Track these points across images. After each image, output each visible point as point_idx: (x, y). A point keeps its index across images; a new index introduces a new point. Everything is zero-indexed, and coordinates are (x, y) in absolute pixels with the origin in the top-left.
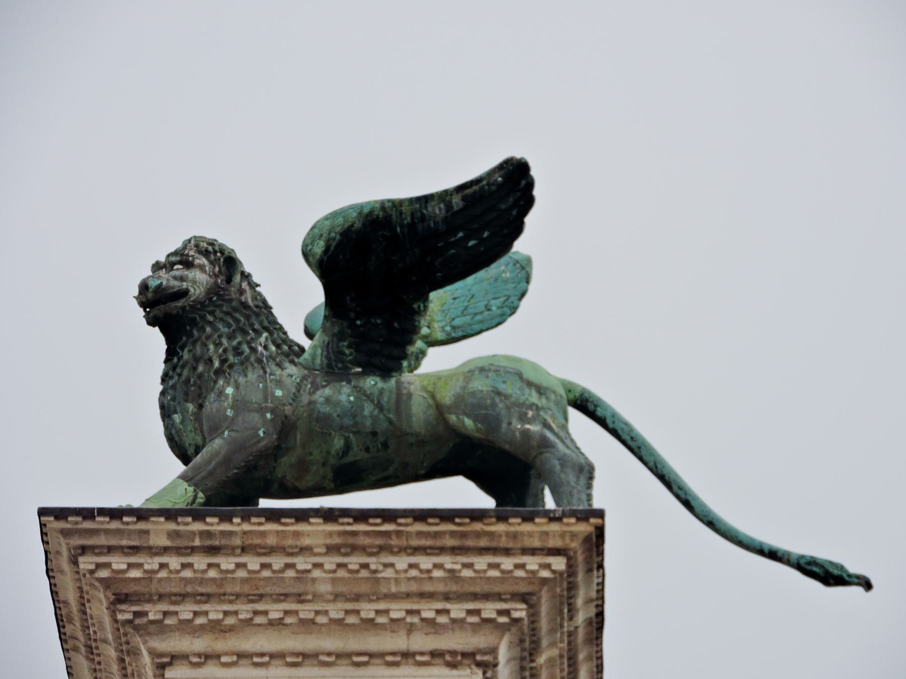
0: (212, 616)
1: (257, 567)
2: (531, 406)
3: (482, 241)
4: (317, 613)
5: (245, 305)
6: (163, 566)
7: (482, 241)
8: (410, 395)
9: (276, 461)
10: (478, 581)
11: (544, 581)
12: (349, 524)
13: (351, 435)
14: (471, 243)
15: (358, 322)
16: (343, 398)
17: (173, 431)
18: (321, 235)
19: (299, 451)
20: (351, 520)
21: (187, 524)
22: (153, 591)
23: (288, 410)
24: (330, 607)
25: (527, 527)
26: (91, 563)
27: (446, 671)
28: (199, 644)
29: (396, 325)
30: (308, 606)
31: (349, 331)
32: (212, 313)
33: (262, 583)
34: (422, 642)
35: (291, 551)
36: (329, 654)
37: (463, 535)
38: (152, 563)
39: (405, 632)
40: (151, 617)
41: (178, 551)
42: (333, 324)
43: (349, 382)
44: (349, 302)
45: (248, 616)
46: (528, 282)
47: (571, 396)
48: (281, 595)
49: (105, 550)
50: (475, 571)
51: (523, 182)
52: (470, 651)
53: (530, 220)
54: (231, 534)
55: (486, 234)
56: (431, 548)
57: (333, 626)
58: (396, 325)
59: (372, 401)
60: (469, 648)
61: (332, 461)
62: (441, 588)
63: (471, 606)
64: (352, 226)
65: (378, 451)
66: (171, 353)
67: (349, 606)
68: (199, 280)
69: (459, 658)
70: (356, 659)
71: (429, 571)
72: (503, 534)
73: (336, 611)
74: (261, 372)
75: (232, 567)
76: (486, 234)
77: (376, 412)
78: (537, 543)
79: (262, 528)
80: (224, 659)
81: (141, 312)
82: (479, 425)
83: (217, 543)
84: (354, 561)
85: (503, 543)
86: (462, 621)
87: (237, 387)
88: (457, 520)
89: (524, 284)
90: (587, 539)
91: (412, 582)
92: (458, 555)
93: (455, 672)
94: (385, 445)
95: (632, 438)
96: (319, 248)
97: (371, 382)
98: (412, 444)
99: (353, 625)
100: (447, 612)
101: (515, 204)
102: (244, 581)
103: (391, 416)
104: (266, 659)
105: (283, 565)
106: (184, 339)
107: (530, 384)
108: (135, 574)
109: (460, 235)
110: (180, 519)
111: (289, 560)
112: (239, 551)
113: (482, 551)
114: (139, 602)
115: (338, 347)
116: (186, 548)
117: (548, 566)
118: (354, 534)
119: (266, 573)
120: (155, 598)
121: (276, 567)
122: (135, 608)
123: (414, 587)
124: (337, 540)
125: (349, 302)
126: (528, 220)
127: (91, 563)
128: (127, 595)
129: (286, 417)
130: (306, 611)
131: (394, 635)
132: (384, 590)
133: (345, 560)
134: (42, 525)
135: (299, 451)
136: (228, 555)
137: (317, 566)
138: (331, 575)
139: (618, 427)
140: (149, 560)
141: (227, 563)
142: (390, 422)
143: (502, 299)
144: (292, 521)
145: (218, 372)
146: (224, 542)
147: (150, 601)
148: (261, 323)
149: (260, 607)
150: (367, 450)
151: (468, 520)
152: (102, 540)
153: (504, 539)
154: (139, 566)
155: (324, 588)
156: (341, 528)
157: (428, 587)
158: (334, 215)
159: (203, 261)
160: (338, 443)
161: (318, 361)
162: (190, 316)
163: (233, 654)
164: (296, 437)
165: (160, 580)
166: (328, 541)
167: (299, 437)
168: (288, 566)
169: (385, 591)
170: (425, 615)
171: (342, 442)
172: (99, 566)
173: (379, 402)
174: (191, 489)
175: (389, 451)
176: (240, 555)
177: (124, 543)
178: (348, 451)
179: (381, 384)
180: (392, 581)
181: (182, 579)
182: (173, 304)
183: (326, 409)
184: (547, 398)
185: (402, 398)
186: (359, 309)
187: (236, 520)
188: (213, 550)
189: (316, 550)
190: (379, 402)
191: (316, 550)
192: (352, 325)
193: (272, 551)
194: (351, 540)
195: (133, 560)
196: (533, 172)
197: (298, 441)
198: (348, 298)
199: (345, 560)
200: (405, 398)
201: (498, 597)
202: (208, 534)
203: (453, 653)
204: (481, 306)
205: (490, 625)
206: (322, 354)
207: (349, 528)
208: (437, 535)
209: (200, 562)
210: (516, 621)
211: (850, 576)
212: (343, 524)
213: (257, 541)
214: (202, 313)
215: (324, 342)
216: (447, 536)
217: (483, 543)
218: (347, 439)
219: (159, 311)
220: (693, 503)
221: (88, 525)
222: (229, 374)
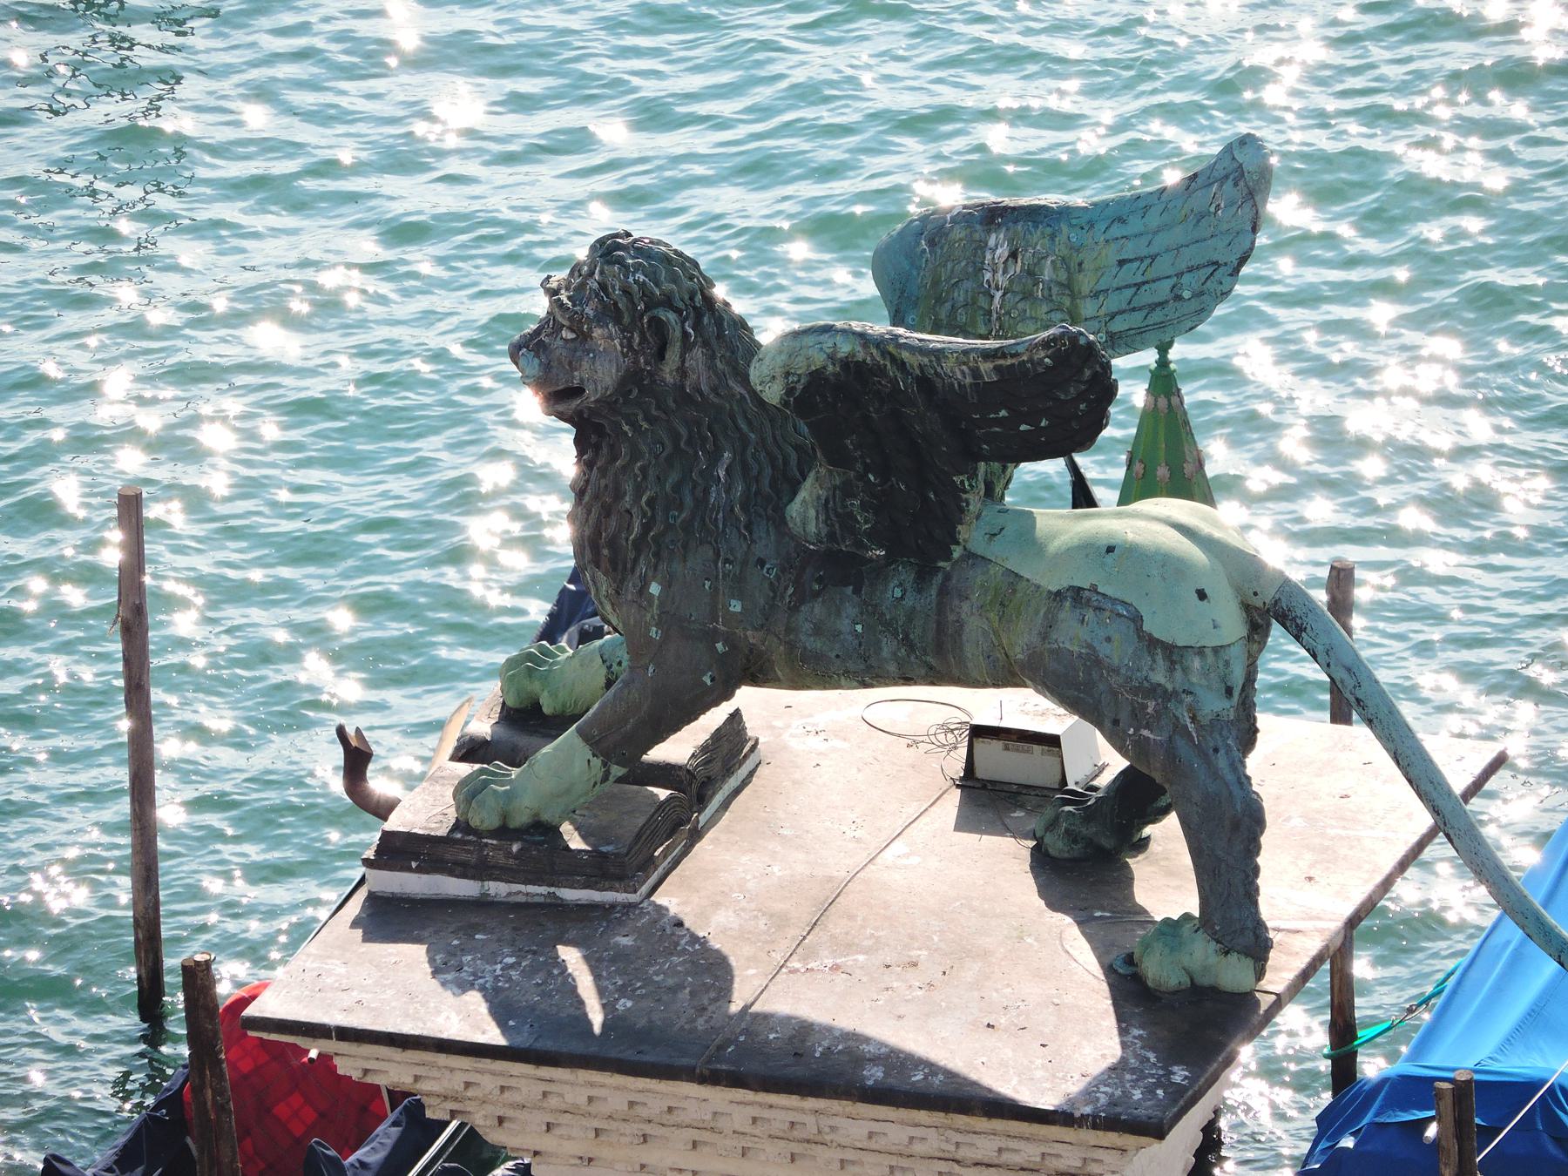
2: (1154, 690)
16: (844, 625)
23: (753, 637)
59: (895, 635)
87: (667, 585)
89: (1250, 235)
103: (929, 659)
161: (812, 528)
173: (906, 637)
174: (597, 762)
190: (906, 637)
215: (819, 498)
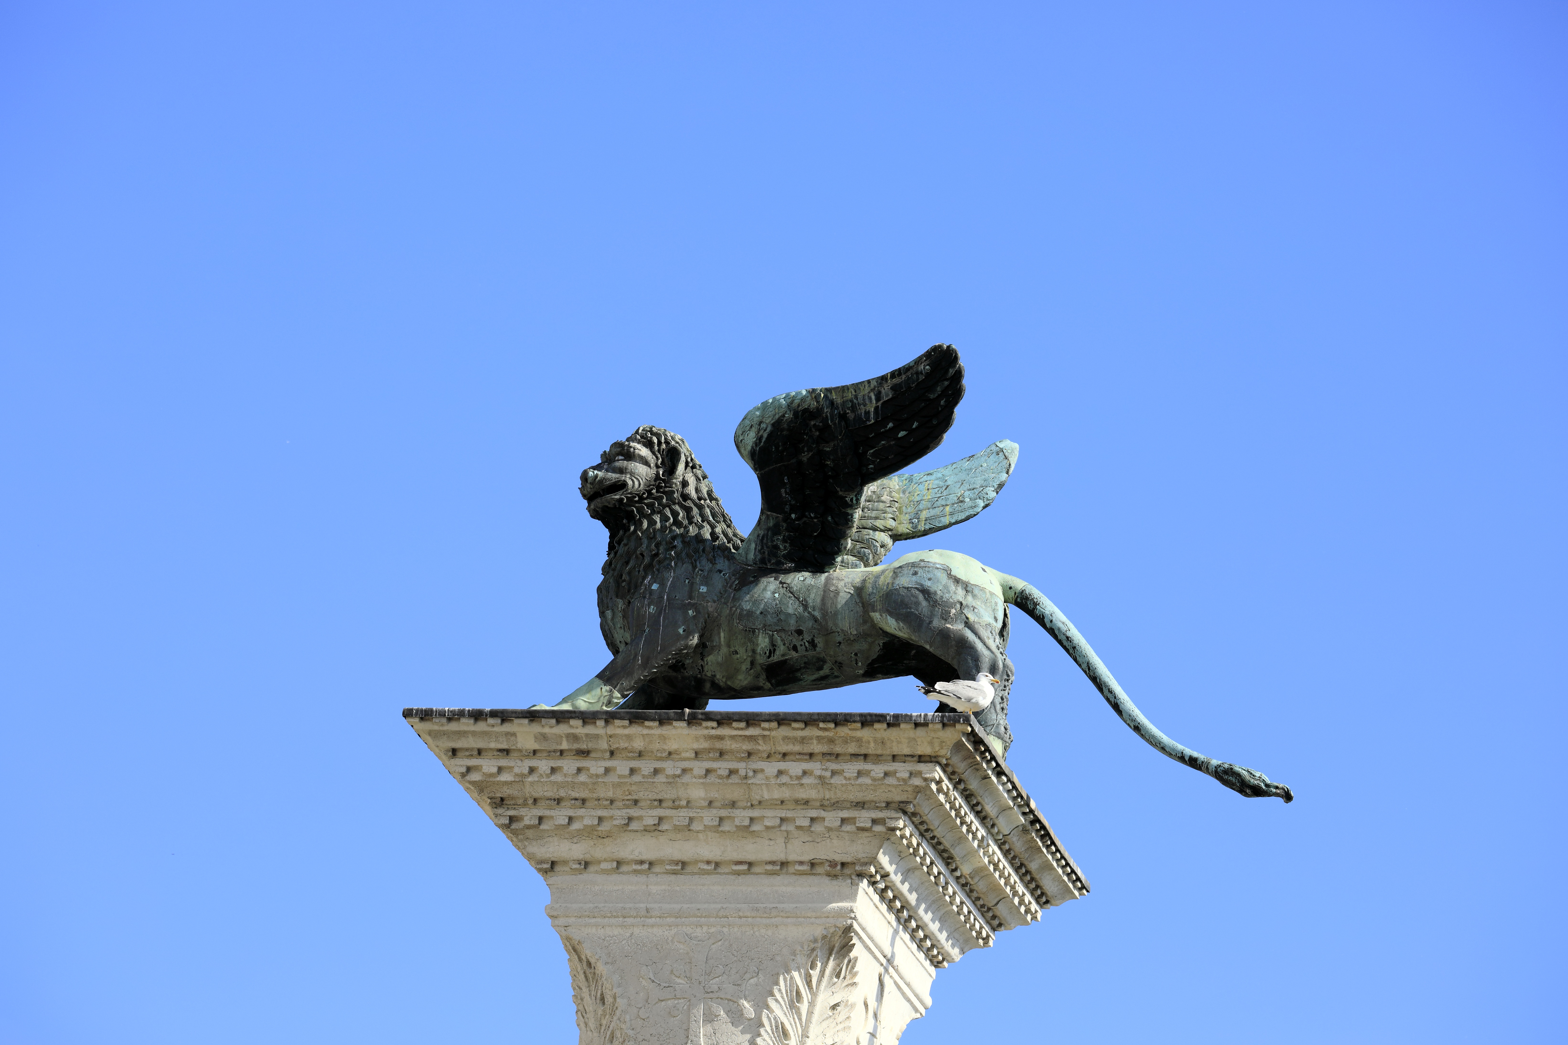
0: (587, 822)
3: (911, 432)
5: (685, 497)
6: (532, 770)
8: (837, 593)
9: (702, 659)
10: (850, 788)
15: (793, 516)
17: (607, 627)
19: (724, 650)
20: (714, 724)
21: (551, 727)
22: (528, 795)
23: (711, 607)
26: (462, 766)
27: (826, 880)
30: (684, 813)
31: (785, 525)
33: (634, 788)
34: (799, 850)
36: (708, 862)
37: (831, 741)
38: (523, 766)
39: (783, 840)
40: (527, 821)
41: (550, 754)
42: (768, 517)
45: (623, 822)
47: (1011, 594)
49: (476, 753)
50: (845, 778)
51: (951, 371)
53: (959, 411)
54: (597, 737)
55: (915, 425)
57: (709, 834)
58: (830, 518)
59: (798, 599)
61: (761, 660)
62: (812, 794)
64: (783, 416)
65: (806, 650)
66: (611, 547)
67: (724, 813)
68: (641, 473)
69: (839, 867)
72: (871, 740)
73: (709, 817)
74: (690, 567)
76: (915, 425)
77: (801, 609)
78: (906, 751)
80: (604, 866)
81: (585, 503)
83: (584, 747)
84: (723, 767)
85: (871, 749)
88: (821, 725)
90: (959, 746)
91: (784, 788)
92: (828, 760)
93: (835, 882)
94: (813, 644)
95: (1068, 638)
96: (750, 438)
98: (840, 643)
99: (729, 832)
100: (823, 819)
102: (616, 786)
104: (646, 866)
105: (652, 770)
106: (621, 532)
107: (957, 581)
108: (505, 777)
109: (890, 425)
111: (658, 765)
112: (608, 754)
114: (515, 806)
116: (555, 751)
118: (721, 738)
119: (636, 778)
120: (530, 802)
122: (512, 813)
123: (786, 793)
124: (705, 745)
126: (956, 410)
127: (462, 766)
128: (502, 799)
130: (680, 816)
131: (772, 843)
132: (756, 797)
135: (724, 650)
136: (596, 759)
137: (684, 771)
138: (701, 781)
140: (519, 763)
141: (596, 767)
142: (816, 620)
145: (649, 567)
146: (590, 746)
147: (525, 804)
148: (702, 515)
149: (634, 812)
150: (795, 648)
154: (510, 768)
155: (698, 793)
156: (706, 732)
157: (802, 794)
158: (765, 405)
159: (644, 451)
160: (763, 642)
161: (751, 556)
162: (629, 509)
163: (613, 860)
164: (719, 634)
165: (532, 783)
166: (696, 746)
167: (722, 635)
168: (656, 772)
170: (798, 823)
171: (767, 640)
175: (817, 649)
177: (493, 745)
178: (775, 650)
180: (764, 787)
181: (555, 783)
184: (974, 596)
187: (600, 723)
188: (584, 753)
189: (684, 755)
192: (787, 519)
193: (640, 754)
194: (719, 745)
195: (503, 762)
196: (962, 362)
197: (722, 639)
200: (832, 595)
202: (575, 738)
203: (833, 864)
204: (953, 498)
205: (866, 834)
206: (755, 549)
207: (713, 732)
208: (803, 740)
209: (569, 765)
211: (1267, 785)
212: (707, 728)
213: (623, 745)
215: (758, 536)
216: (815, 742)
217: (852, 748)
219: (598, 502)
220: (1121, 707)
222: (658, 570)
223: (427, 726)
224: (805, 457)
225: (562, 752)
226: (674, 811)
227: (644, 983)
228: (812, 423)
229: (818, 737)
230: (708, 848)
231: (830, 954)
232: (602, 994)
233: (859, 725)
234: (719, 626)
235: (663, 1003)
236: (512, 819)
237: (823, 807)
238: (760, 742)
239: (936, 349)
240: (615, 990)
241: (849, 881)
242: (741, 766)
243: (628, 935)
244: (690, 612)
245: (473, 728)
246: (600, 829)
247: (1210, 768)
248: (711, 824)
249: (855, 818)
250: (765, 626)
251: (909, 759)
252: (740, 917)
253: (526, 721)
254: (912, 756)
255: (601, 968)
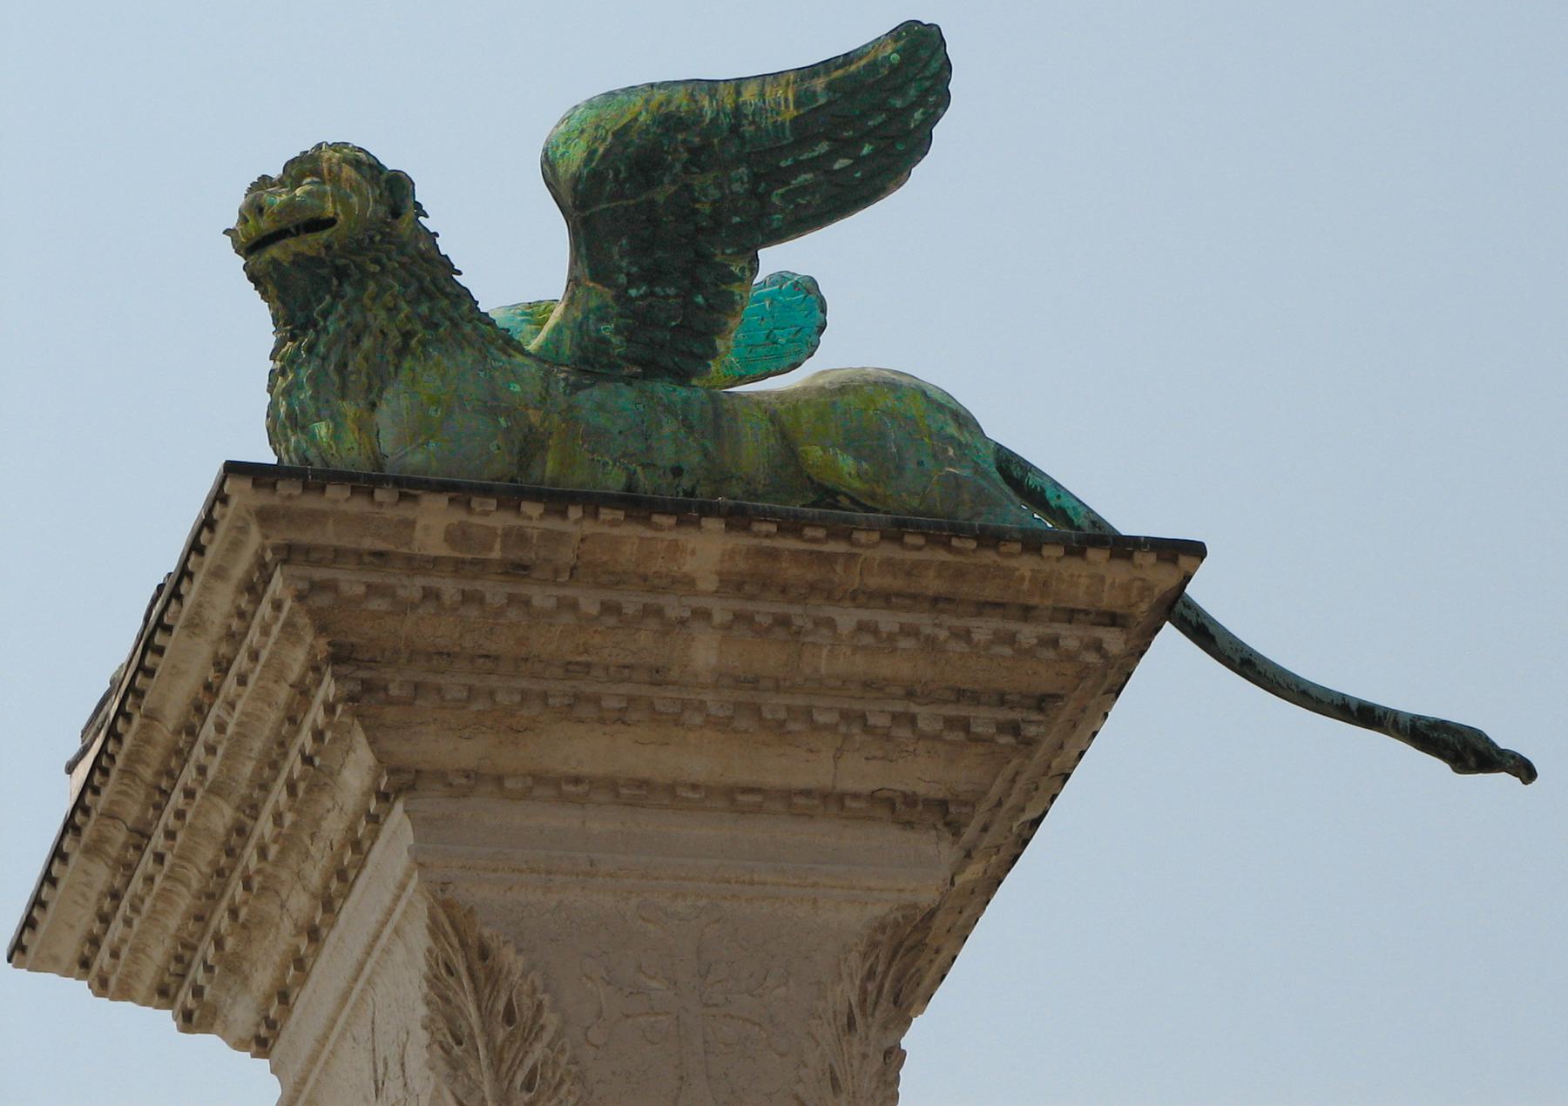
1: (594, 610)
2: (951, 439)
4: (685, 704)
6: (430, 595)
7: (859, 161)
11: (1084, 671)
12: (767, 536)
13: (639, 469)
14: (840, 164)
15: (633, 292)
18: (582, 131)
21: (486, 514)
23: (534, 417)
24: (708, 697)
25: (1074, 566)
28: (468, 751)
29: (700, 299)
31: (617, 309)
32: (377, 261)
33: (597, 639)
34: (861, 773)
35: (656, 582)
36: (694, 787)
37: (960, 574)
41: (458, 566)
43: (629, 384)
44: (616, 257)
46: (824, 311)
48: (625, 667)
51: (935, 65)
52: (940, 795)
54: (558, 538)
55: (867, 150)
56: (899, 595)
58: (700, 299)
60: (939, 793)
63: (951, 711)
64: (636, 119)
67: (741, 696)
69: (920, 807)
70: (741, 798)
71: (891, 637)
75: (551, 603)
76: (867, 150)
78: (1080, 599)
79: (616, 531)
82: (865, 466)
83: (528, 556)
84: (765, 609)
86: (936, 737)
88: (955, 542)
92: (942, 611)
96: (576, 154)
97: (662, 388)
101: (920, 102)
103: (708, 443)
104: (582, 789)
106: (328, 298)
107: (941, 407)
109: (823, 147)
110: (476, 503)
111: (649, 599)
112: (565, 577)
113: (983, 607)
115: (598, 330)
116: (473, 562)
117: (1098, 646)
118: (773, 554)
121: (629, 610)
122: (362, 674)
123: (859, 665)
124: (742, 565)
125: (616, 257)
129: (531, 427)
133: (750, 606)
134: (219, 497)
136: (543, 582)
139: (1066, 503)
140: (406, 581)
141: (542, 598)
143: (793, 330)
144: (672, 521)
151: (972, 544)
152: (327, 535)
153: (1026, 585)
156: (755, 542)
157: (886, 667)
162: (341, 262)
167: (550, 465)
169: (807, 671)
171: (623, 480)
172: (316, 587)
176: (563, 585)
177: (368, 543)
179: (683, 392)
180: (825, 651)
182: (310, 237)
183: (602, 420)
185: (719, 419)
186: (634, 270)
187: (575, 512)
188: (518, 570)
190: (685, 419)
191: (702, 585)
195: (375, 578)
198: (615, 250)
199: (750, 606)
201: (1002, 700)
202: (521, 537)
203: (910, 800)
205: (980, 749)
207: (767, 543)
208: (912, 571)
209: (495, 590)
210: (1029, 743)
212: (757, 535)
214: (359, 259)
217: (991, 592)
218: (631, 475)
220: (1212, 630)
221: (310, 502)
223: (263, 499)
224: (660, 196)
225: (484, 563)
226: (655, 689)
227: (589, 985)
228: (680, 137)
229: (943, 563)
230: (696, 759)
231: (893, 959)
232: (509, 1004)
233: (1017, 547)
234: (544, 448)
235: (630, 1021)
236: (368, 687)
237: (910, 695)
238: (839, 569)
239: (910, 25)
240: (539, 996)
241: (933, 833)
242: (795, 610)
243: (553, 904)
244: (502, 421)
245: (343, 507)
246: (524, 712)
247: (1401, 720)
248: (721, 714)
249: (967, 718)
250: (624, 455)
251: (1082, 617)
252: (752, 883)
253: (442, 501)
254: (1087, 612)
255: (510, 959)
